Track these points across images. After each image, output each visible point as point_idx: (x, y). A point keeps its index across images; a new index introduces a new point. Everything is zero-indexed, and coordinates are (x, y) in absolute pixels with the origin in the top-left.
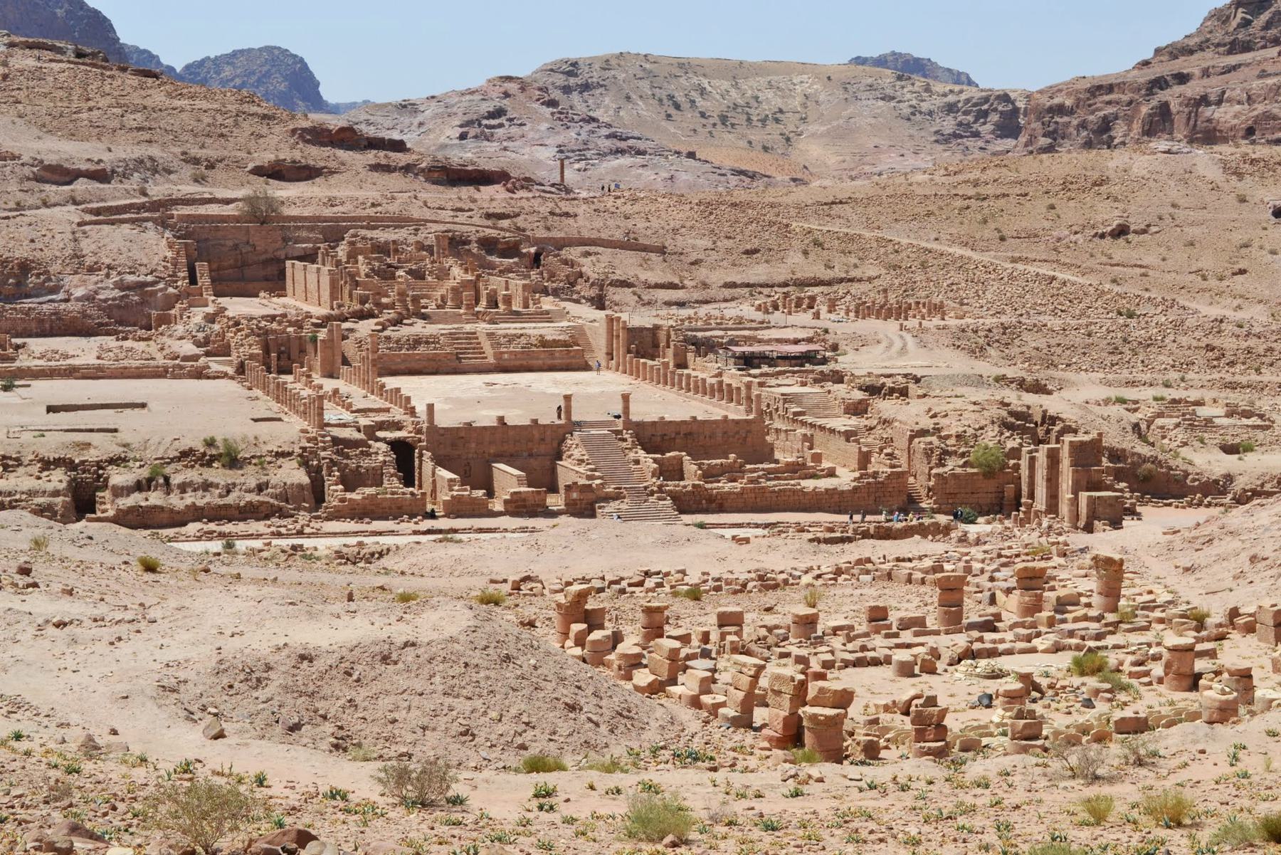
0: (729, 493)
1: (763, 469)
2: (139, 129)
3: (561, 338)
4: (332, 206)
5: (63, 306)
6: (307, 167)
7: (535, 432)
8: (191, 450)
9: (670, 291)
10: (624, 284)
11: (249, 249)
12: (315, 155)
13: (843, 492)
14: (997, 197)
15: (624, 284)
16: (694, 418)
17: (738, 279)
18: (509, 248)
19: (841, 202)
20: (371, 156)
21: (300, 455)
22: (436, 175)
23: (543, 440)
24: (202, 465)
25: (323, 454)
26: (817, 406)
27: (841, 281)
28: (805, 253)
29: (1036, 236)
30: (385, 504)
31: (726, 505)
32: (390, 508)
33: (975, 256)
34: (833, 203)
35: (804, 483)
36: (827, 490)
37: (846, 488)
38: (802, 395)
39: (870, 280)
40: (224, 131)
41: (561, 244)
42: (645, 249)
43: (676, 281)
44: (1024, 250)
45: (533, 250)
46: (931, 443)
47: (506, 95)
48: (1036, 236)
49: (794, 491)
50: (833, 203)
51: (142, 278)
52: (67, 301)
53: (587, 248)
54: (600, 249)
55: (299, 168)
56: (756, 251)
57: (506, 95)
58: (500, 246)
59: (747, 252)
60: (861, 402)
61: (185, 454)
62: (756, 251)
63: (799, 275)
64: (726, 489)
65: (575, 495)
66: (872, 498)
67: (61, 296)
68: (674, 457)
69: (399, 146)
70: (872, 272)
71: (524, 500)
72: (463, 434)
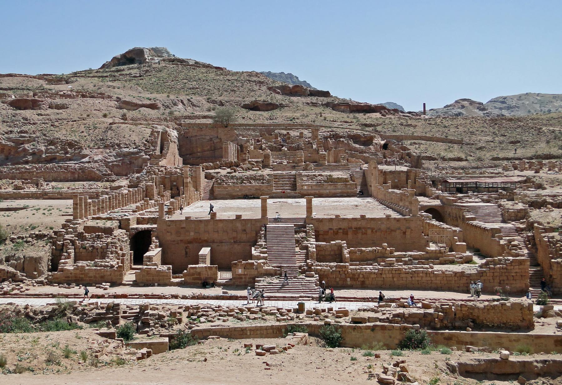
0: (370, 273)
1: (411, 256)
2: (193, 88)
4: (271, 119)
5: (86, 165)
6: (271, 104)
7: (239, 225)
9: (456, 162)
10: (430, 158)
11: (218, 140)
12: (279, 98)
13: (470, 275)
15: (430, 158)
16: (363, 217)
17: (501, 155)
18: (368, 140)
20: (309, 99)
22: (343, 108)
23: (245, 230)
25: (67, 237)
26: (488, 215)
30: (91, 274)
31: (367, 282)
32: (95, 277)
35: (437, 267)
36: (456, 273)
37: (474, 272)
38: (479, 207)
40: (235, 89)
41: (399, 139)
42: (451, 142)
43: (463, 157)
45: (383, 142)
46: (553, 237)
47: (463, 107)
49: (427, 273)
51: (132, 150)
52: (89, 162)
53: (413, 141)
54: (423, 142)
55: (267, 104)
57: (463, 107)
58: (362, 139)
59: (512, 142)
64: (368, 270)
65: (240, 271)
66: (497, 280)
67: (87, 159)
68: (335, 244)
69: (326, 94)
71: (199, 274)
72: (184, 225)
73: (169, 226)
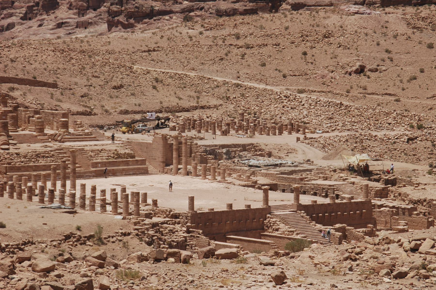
3: (127, 151)
8: (72, 234)
14: (260, 46)
19: (154, 50)
21: (137, 235)
24: (81, 244)
27: (196, 108)
28: (154, 87)
29: (306, 74)
33: (269, 87)
34: (149, 51)
39: (216, 107)
44: (302, 84)
48: (306, 74)
50: (149, 51)
53: (11, 85)
56: (121, 86)
60: (383, 189)
61: (67, 237)
62: (121, 86)
63: (165, 105)
70: (214, 102)
72: (211, 217)
73: (200, 218)
